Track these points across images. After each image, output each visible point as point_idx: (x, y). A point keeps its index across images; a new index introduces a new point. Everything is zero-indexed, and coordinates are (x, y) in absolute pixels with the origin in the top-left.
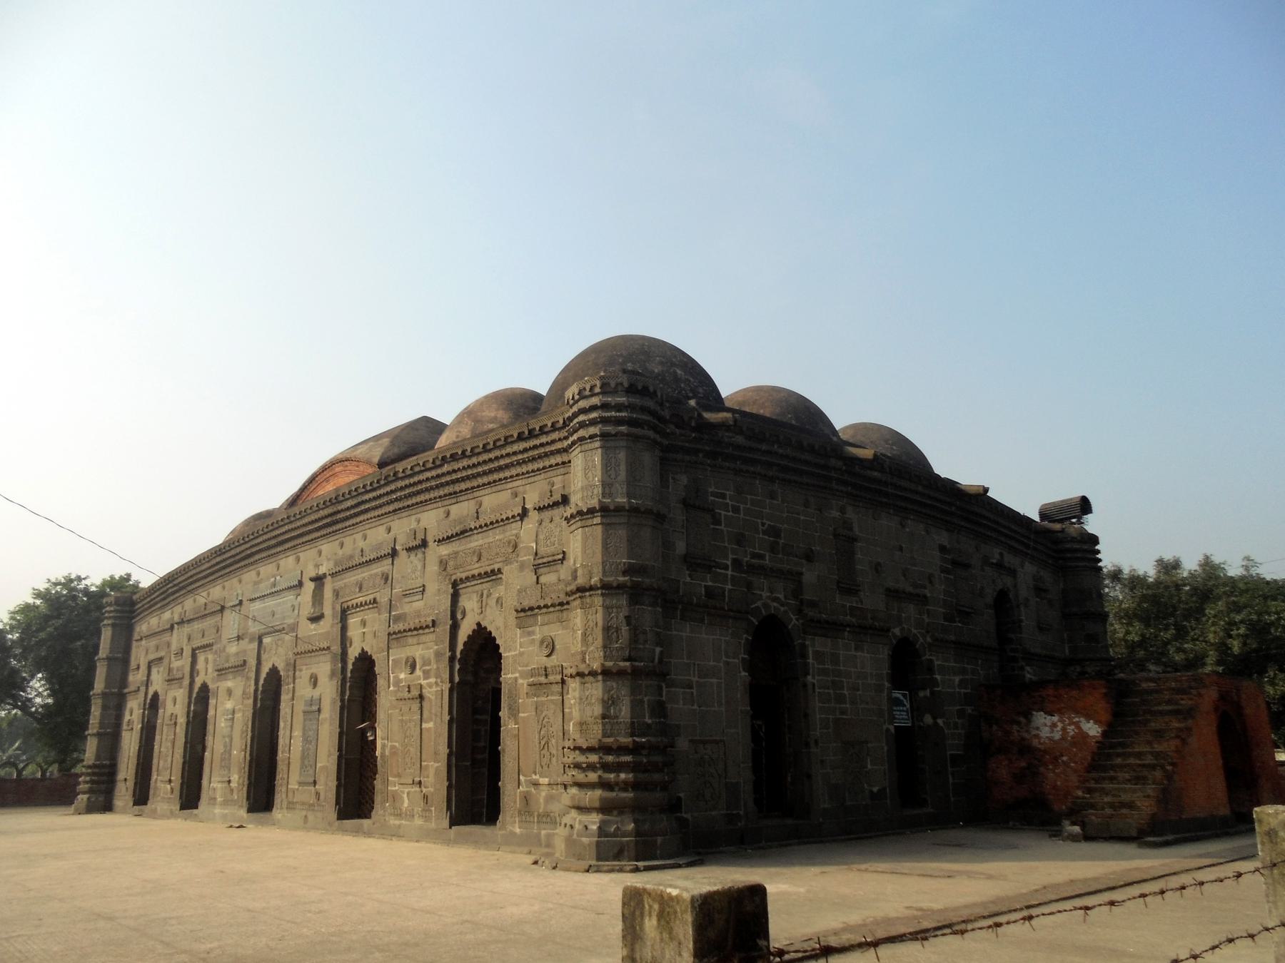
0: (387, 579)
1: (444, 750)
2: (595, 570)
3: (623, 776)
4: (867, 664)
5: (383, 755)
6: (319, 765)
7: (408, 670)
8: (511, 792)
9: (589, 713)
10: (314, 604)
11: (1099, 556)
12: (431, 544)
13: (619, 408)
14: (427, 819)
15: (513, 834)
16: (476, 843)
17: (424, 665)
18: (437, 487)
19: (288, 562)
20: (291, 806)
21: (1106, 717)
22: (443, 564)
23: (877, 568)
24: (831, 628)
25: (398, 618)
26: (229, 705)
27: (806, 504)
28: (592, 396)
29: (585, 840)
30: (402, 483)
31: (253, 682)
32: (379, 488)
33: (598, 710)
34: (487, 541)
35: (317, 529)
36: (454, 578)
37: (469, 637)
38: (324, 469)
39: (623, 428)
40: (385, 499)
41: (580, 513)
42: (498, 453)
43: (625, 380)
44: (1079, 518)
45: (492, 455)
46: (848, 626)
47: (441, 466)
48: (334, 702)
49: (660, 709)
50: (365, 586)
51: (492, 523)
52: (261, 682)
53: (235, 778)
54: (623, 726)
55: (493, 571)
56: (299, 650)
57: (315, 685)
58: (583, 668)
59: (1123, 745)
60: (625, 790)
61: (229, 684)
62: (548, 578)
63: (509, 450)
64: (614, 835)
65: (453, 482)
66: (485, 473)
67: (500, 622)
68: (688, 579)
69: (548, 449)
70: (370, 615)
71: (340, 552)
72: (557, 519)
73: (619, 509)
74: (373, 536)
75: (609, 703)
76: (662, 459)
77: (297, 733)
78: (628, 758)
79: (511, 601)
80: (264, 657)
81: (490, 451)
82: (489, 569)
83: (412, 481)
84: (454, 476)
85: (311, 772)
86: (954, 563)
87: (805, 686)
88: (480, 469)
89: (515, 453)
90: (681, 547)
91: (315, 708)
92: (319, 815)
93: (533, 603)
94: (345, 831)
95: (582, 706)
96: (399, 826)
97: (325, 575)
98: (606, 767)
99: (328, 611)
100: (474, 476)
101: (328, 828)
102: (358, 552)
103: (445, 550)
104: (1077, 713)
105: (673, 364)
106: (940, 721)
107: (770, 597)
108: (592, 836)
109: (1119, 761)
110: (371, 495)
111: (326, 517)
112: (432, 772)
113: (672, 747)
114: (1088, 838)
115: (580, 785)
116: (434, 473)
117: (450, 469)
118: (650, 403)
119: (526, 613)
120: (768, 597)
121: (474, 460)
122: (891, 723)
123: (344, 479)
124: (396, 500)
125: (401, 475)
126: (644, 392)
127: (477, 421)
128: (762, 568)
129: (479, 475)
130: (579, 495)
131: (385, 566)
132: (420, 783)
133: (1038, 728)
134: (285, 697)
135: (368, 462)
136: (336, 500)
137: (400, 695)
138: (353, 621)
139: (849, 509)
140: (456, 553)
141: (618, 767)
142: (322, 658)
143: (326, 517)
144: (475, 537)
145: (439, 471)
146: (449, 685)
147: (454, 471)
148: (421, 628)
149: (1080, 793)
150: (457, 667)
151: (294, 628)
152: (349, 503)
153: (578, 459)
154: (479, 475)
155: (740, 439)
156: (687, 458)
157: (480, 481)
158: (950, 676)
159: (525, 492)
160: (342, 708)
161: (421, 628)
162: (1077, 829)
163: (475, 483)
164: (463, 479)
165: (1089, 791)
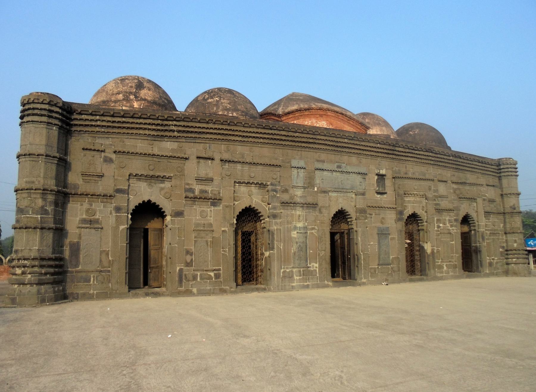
6: (391, 257)
10: (378, 186)
26: (300, 225)
53: (315, 266)
61: (298, 213)
96: (442, 276)
103: (455, 186)
119: (487, 214)
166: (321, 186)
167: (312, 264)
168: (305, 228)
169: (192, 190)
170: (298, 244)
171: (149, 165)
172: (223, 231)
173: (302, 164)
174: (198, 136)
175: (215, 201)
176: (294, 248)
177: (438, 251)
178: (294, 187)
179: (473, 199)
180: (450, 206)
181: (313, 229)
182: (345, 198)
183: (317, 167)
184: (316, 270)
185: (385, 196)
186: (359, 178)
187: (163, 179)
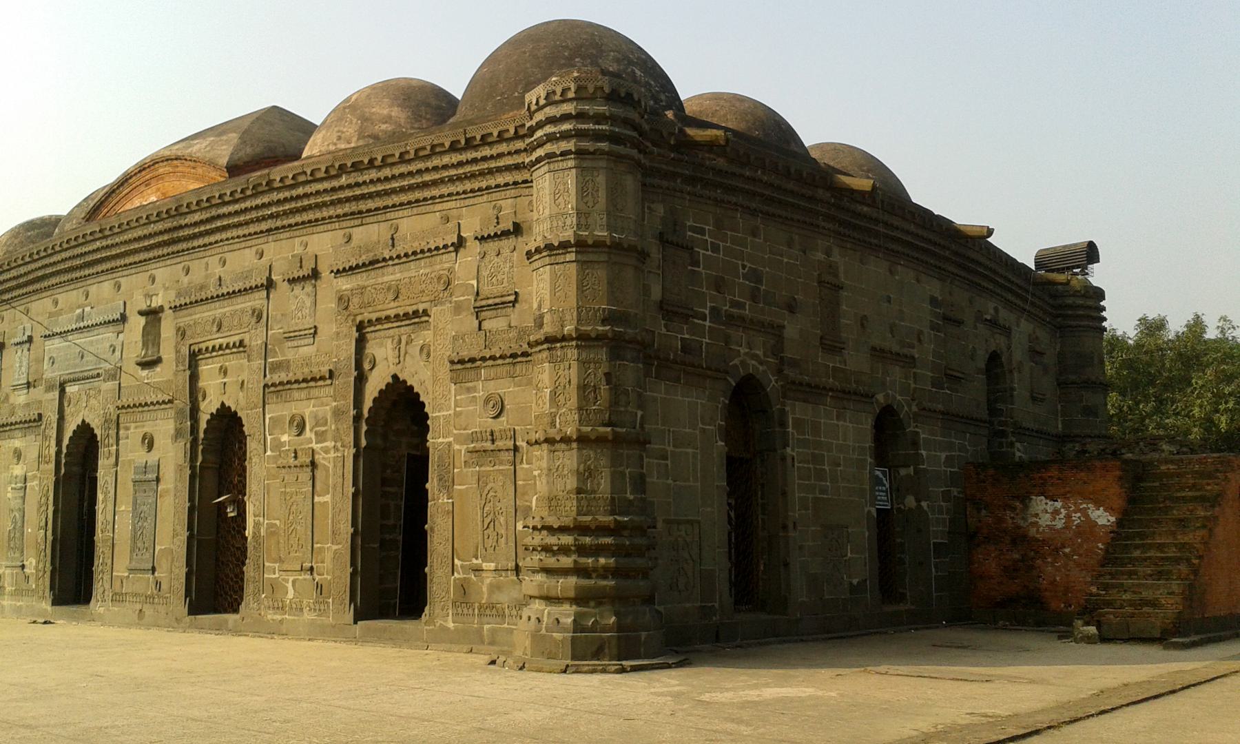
0: (259, 317)
1: (346, 529)
2: (568, 317)
3: (602, 561)
4: (850, 433)
5: (256, 535)
6: (157, 548)
7: (294, 431)
8: (441, 578)
9: (559, 485)
10: (145, 344)
11: (1104, 314)
12: (325, 273)
13: (598, 118)
14: (322, 613)
15: (444, 629)
16: (394, 641)
17: (317, 425)
18: (333, 203)
19: (102, 289)
20: (118, 598)
21: (1119, 503)
22: (343, 301)
23: (863, 322)
24: (812, 392)
25: (277, 367)
27: (790, 244)
28: (563, 102)
29: (556, 635)
30: (281, 196)
31: (53, 443)
32: (244, 199)
33: (572, 483)
34: (406, 274)
35: (147, 249)
36: (359, 318)
37: (381, 392)
38: (142, 168)
39: (604, 145)
40: (254, 215)
41: (549, 247)
42: (421, 165)
43: (606, 84)
44: (1084, 268)
45: (413, 167)
46: (831, 390)
47: (338, 176)
48: (180, 469)
49: (640, 483)
50: (225, 324)
51: (414, 253)
52: (66, 442)
54: (601, 502)
55: (416, 313)
56: (124, 401)
57: (150, 446)
58: (553, 433)
59: (1142, 536)
60: (605, 577)
62: (494, 324)
63: (436, 162)
64: (592, 629)
65: (356, 198)
66: (402, 190)
67: (426, 374)
68: (664, 331)
69: (493, 164)
70: (232, 362)
71: (185, 280)
72: (506, 252)
73: (598, 244)
74: (239, 261)
75: (585, 475)
76: (644, 185)
77: (124, 507)
78: (608, 540)
79: (444, 350)
80: (68, 411)
81: (409, 161)
82: (410, 310)
83: (294, 193)
84: (358, 192)
85: (148, 556)
86: (946, 318)
87: (784, 459)
88: (395, 185)
89: (445, 167)
90: (656, 293)
91: (152, 476)
92: (162, 609)
93: (475, 353)
94: (201, 628)
95: (546, 482)
96: (281, 621)
97: (161, 309)
98: (582, 550)
99: (167, 351)
100: (387, 193)
101: (174, 625)
102: (213, 281)
104: (1087, 498)
105: (630, 63)
106: (924, 504)
107: (749, 355)
108: (565, 630)
109: (1137, 553)
110: (231, 208)
111: (161, 233)
112: (328, 556)
113: (654, 527)
114: (1104, 639)
115: (548, 571)
116: (327, 185)
117: (352, 181)
118: (633, 115)
119: (464, 366)
120: (746, 354)
121: (387, 172)
122: (873, 505)
123: (185, 185)
124: (271, 216)
125: (277, 185)
126: (628, 100)
127: (365, 119)
128: (742, 318)
129: (394, 191)
130: (547, 225)
131: (257, 300)
132: (312, 569)
133: (1037, 515)
134: (104, 465)
135: (212, 164)
136: (177, 210)
137: (281, 462)
138: (208, 369)
139: (836, 251)
140: (364, 287)
141: (597, 551)
142: (160, 414)
143: (161, 233)
144: (391, 269)
145: (335, 183)
146: (353, 451)
147: (358, 185)
148: (314, 379)
149: (1094, 590)
150: (364, 428)
151: (115, 374)
152: (197, 217)
153: (543, 181)
154: (394, 191)
155: (721, 163)
156: (665, 183)
157: (396, 199)
158: (937, 452)
159: (459, 217)
160: (192, 477)
161: (314, 379)
162: (1092, 630)
163: (389, 201)
164: (371, 196)
165: (1106, 587)
185: (158, 369)
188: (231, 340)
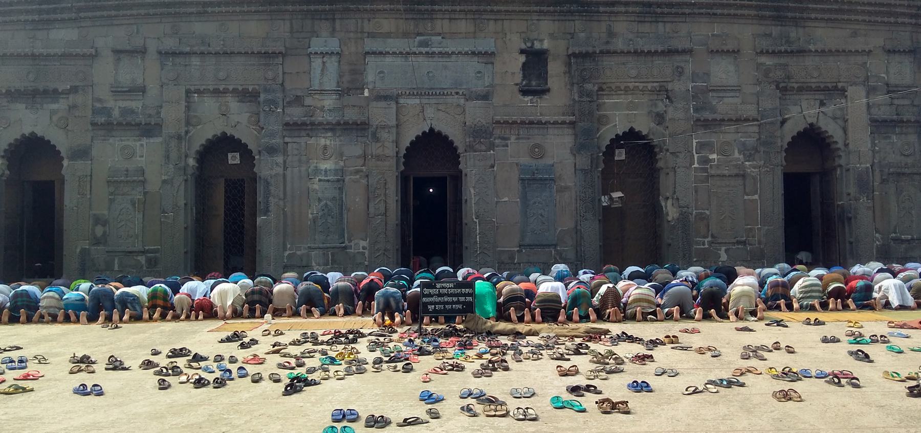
10: (524, 77)
36: (782, 85)
55: (836, 88)
61: (323, 141)
82: (829, 85)
161: (747, 120)
166: (379, 85)
167: (356, 241)
168: (341, 172)
169: (107, 111)
170: (323, 203)
171: (29, 73)
172: (164, 182)
173: (333, 45)
174: (113, 13)
175: (148, 130)
176: (314, 210)
177: (701, 217)
178: (311, 92)
179: (835, 91)
180: (750, 110)
181: (357, 172)
182: (440, 107)
183: (367, 49)
184: (363, 254)
186: (474, 64)
187: (53, 94)
188: (649, 86)
